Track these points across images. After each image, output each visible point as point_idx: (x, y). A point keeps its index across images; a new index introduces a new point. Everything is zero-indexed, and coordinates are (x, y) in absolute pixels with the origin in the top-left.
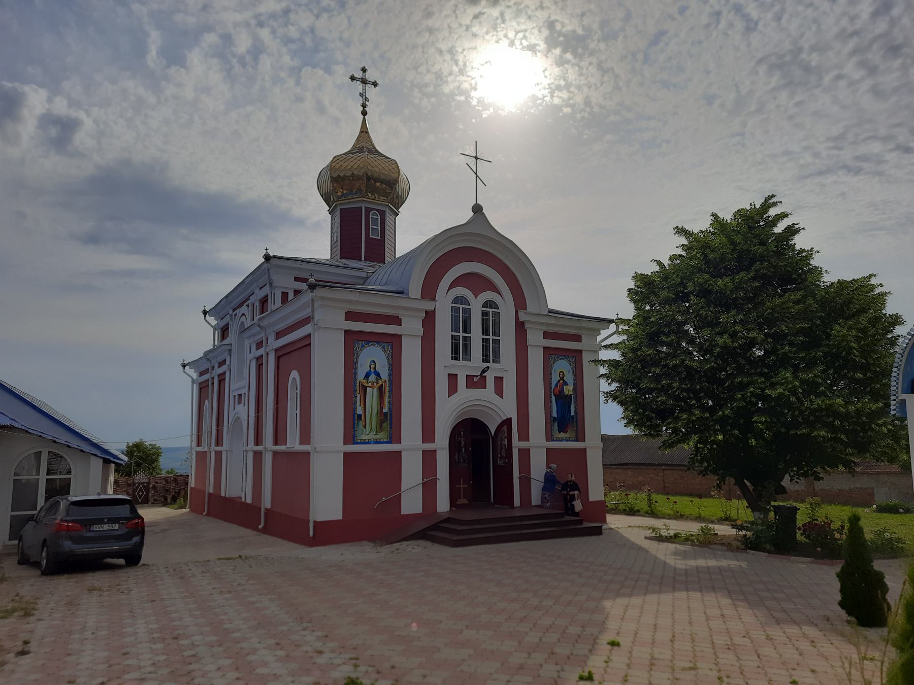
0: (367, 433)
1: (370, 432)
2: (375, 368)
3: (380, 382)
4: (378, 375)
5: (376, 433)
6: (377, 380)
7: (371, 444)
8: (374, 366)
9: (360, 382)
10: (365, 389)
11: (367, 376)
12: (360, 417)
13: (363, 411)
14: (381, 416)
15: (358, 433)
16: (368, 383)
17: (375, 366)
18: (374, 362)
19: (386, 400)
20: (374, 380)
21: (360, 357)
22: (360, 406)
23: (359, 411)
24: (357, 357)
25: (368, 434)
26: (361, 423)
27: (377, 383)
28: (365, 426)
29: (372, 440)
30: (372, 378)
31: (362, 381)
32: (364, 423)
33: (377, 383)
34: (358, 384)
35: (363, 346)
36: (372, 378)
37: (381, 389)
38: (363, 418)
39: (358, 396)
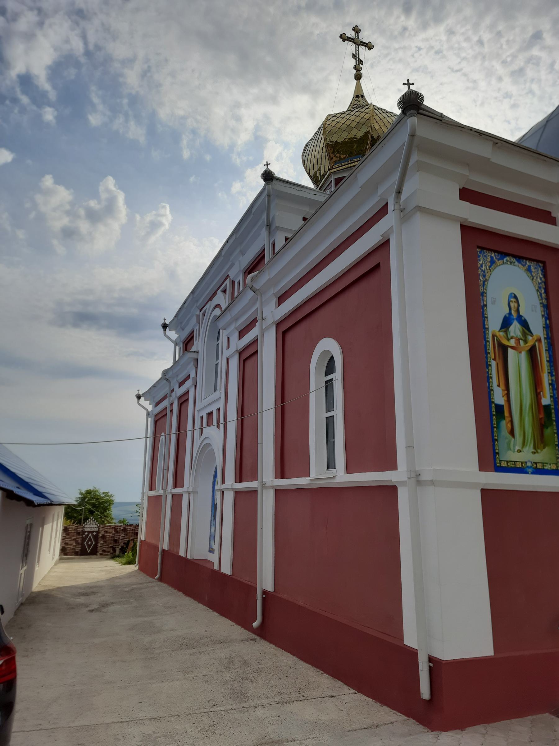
0: (517, 448)
1: (524, 444)
2: (518, 311)
3: (531, 340)
4: (524, 324)
5: (535, 448)
6: (524, 334)
7: (526, 473)
8: (516, 305)
9: (494, 336)
10: (503, 350)
11: (506, 324)
12: (500, 408)
13: (505, 398)
14: (539, 413)
15: (501, 446)
16: (508, 340)
17: (519, 305)
18: (515, 297)
19: (546, 379)
20: (519, 334)
21: (490, 282)
22: (499, 386)
23: (499, 398)
24: (484, 282)
25: (520, 451)
26: (504, 425)
27: (526, 342)
28: (512, 433)
29: (529, 464)
30: (515, 329)
31: (498, 334)
32: (509, 425)
33: (526, 342)
34: (490, 339)
35: (492, 262)
36: (515, 329)
37: (532, 353)
38: (506, 414)
39: (494, 363)
